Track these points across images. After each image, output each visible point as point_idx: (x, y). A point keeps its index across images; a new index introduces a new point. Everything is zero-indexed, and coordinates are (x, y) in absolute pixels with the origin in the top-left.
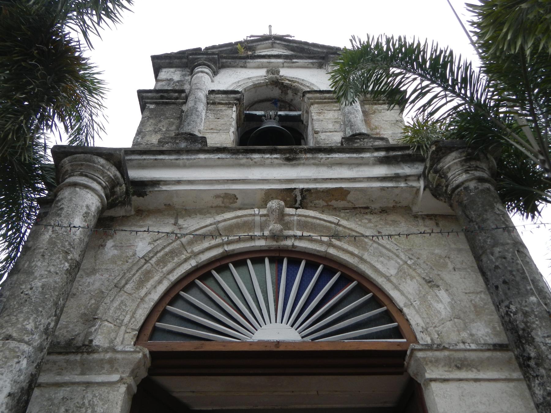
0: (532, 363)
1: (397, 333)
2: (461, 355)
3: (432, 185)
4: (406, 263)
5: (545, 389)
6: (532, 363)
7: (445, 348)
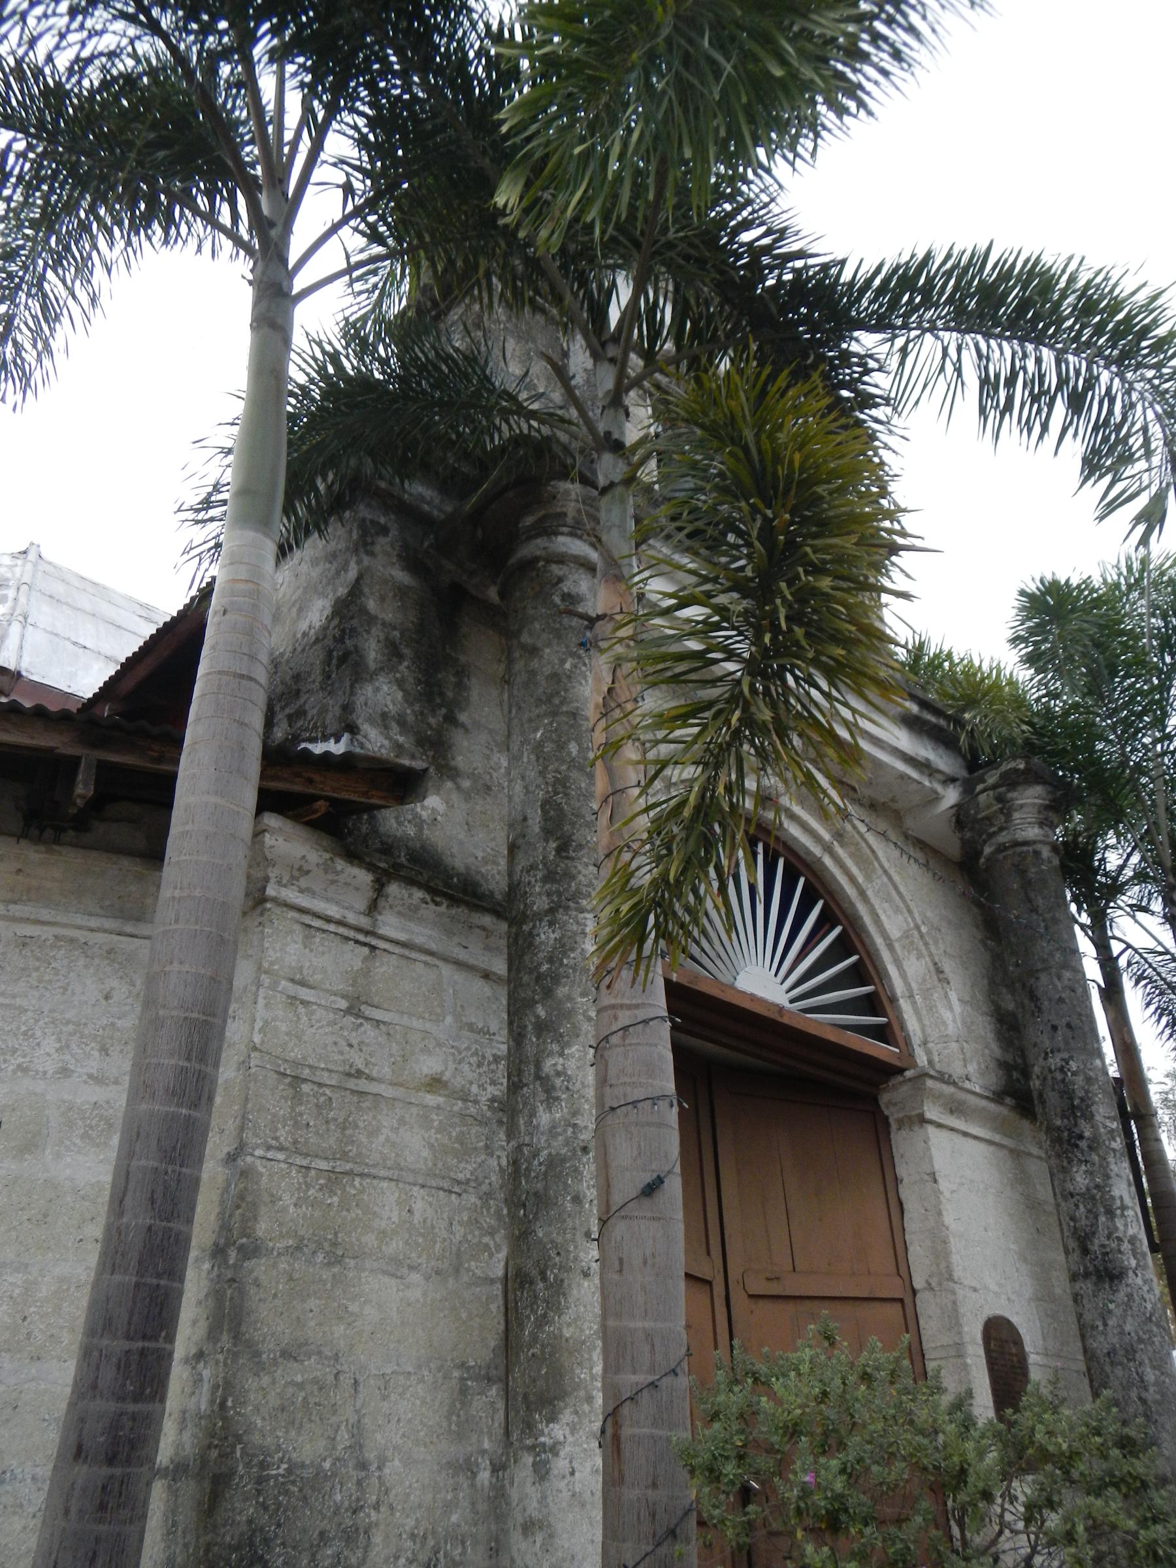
0: (1083, 1144)
1: (882, 1033)
2: (962, 1096)
3: (977, 813)
4: (918, 927)
5: (1092, 1180)
6: (1083, 1144)
7: (954, 1084)
